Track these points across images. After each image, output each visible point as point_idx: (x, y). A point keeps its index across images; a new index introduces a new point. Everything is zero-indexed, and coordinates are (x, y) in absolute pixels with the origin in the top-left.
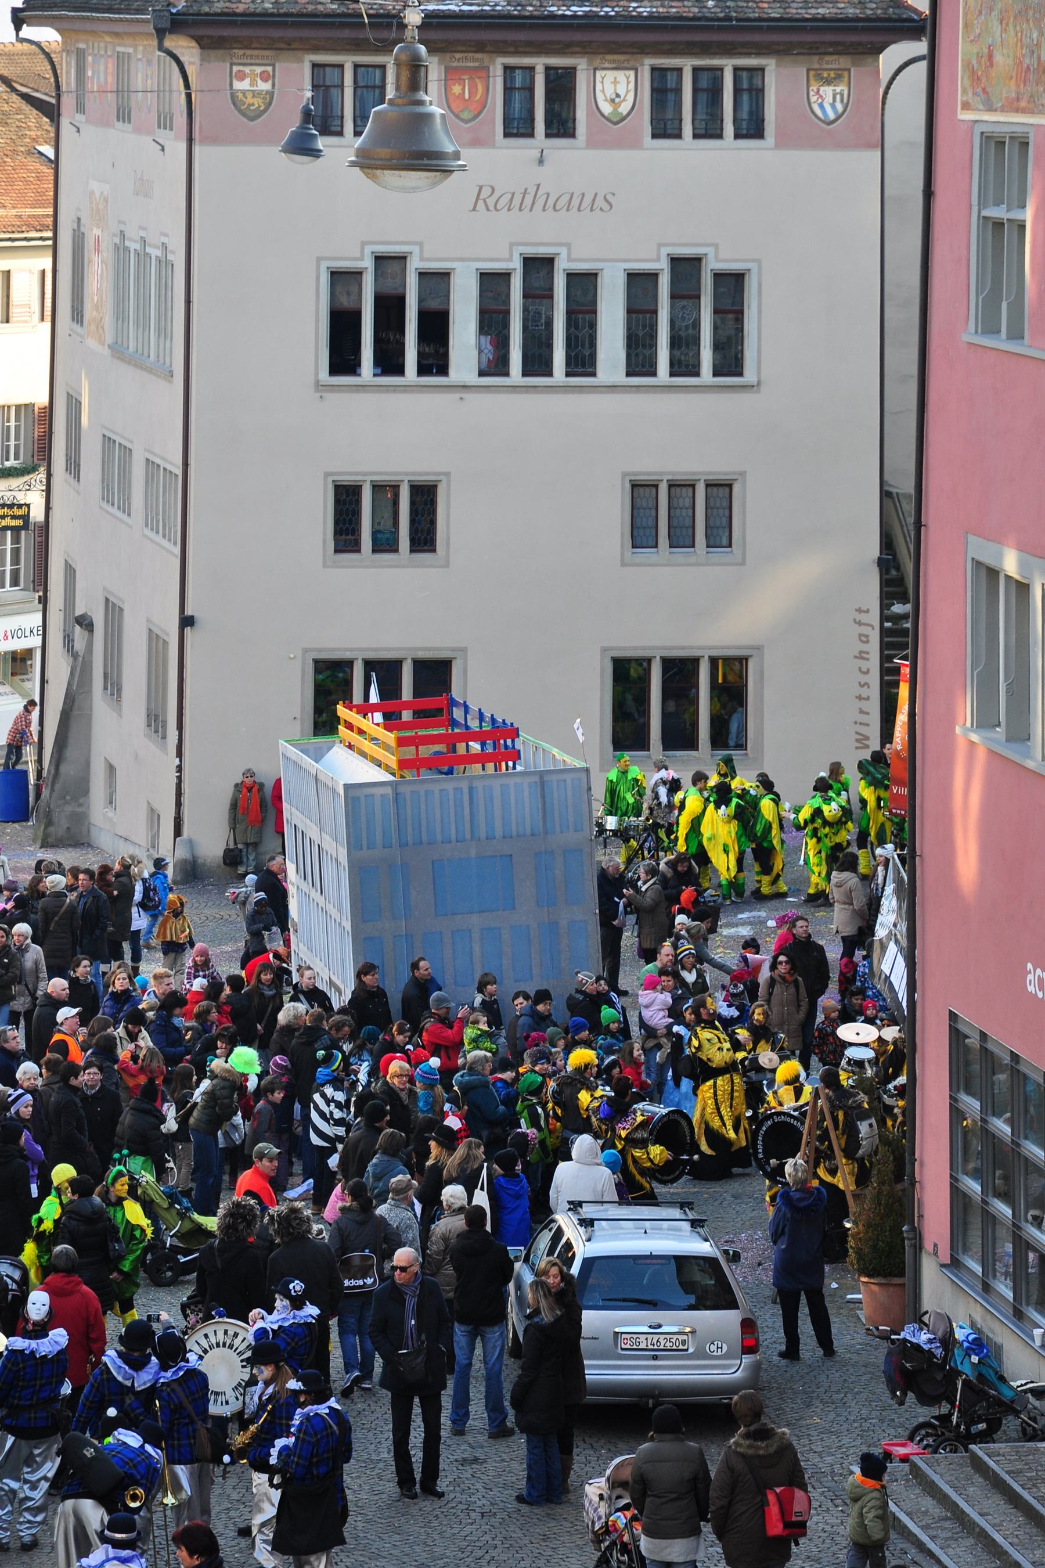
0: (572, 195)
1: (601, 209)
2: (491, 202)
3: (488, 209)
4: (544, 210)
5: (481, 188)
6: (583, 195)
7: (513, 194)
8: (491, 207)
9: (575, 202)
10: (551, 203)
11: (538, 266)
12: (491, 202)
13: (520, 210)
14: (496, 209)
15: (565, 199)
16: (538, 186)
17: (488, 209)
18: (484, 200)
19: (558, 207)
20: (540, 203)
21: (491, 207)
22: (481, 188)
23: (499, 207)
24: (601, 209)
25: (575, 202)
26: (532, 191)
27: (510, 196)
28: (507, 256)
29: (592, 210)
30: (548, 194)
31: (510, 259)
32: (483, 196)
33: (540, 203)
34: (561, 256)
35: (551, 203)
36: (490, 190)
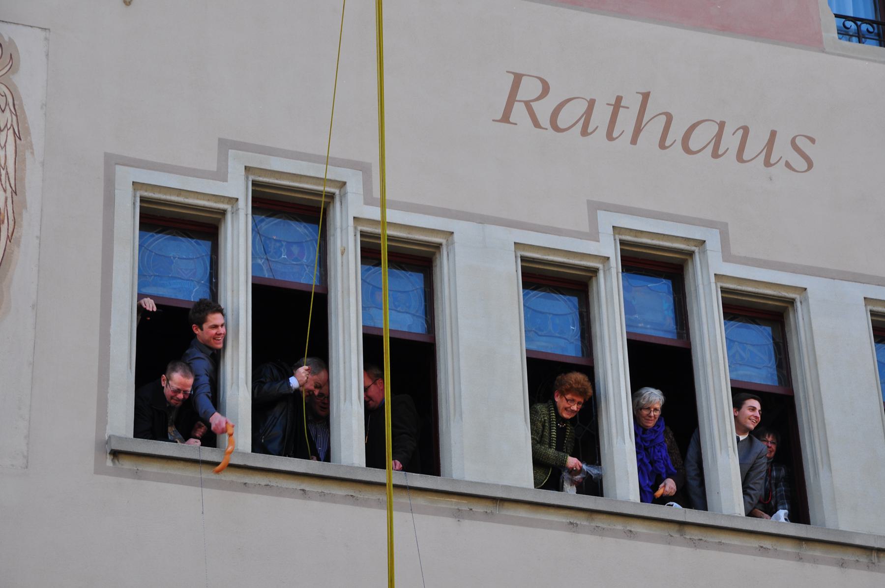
0: (722, 125)
1: (788, 165)
2: (543, 109)
3: (537, 124)
4: (662, 146)
5: (518, 79)
6: (746, 130)
7: (592, 103)
8: (545, 121)
9: (731, 141)
10: (676, 133)
11: (658, 266)
12: (543, 109)
13: (610, 137)
14: (556, 129)
15: (702, 137)
16: (646, 96)
17: (537, 124)
18: (528, 104)
19: (693, 145)
20: (653, 130)
21: (545, 121)
22: (518, 79)
23: (563, 120)
24: (788, 165)
25: (731, 141)
26: (633, 103)
27: (585, 105)
28: (585, 227)
29: (767, 163)
30: (669, 118)
31: (593, 235)
32: (522, 95)
33: (653, 130)
34: (708, 245)
35: (676, 133)
36: (538, 88)
